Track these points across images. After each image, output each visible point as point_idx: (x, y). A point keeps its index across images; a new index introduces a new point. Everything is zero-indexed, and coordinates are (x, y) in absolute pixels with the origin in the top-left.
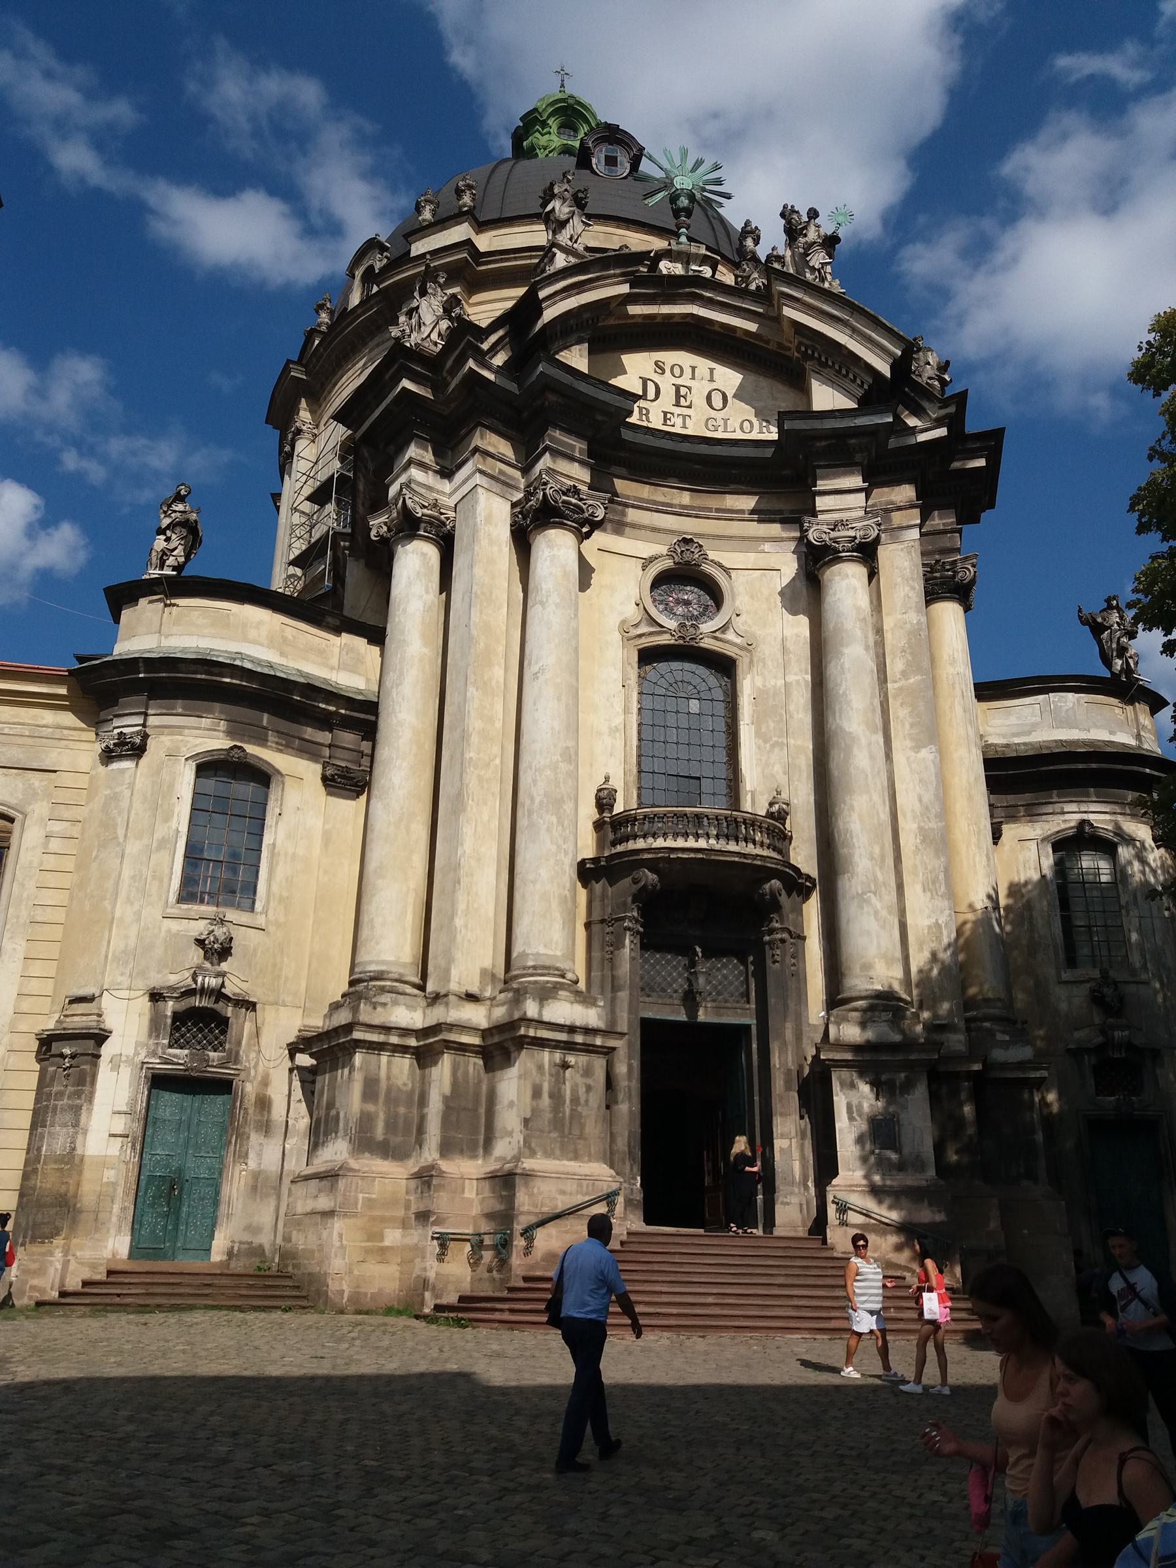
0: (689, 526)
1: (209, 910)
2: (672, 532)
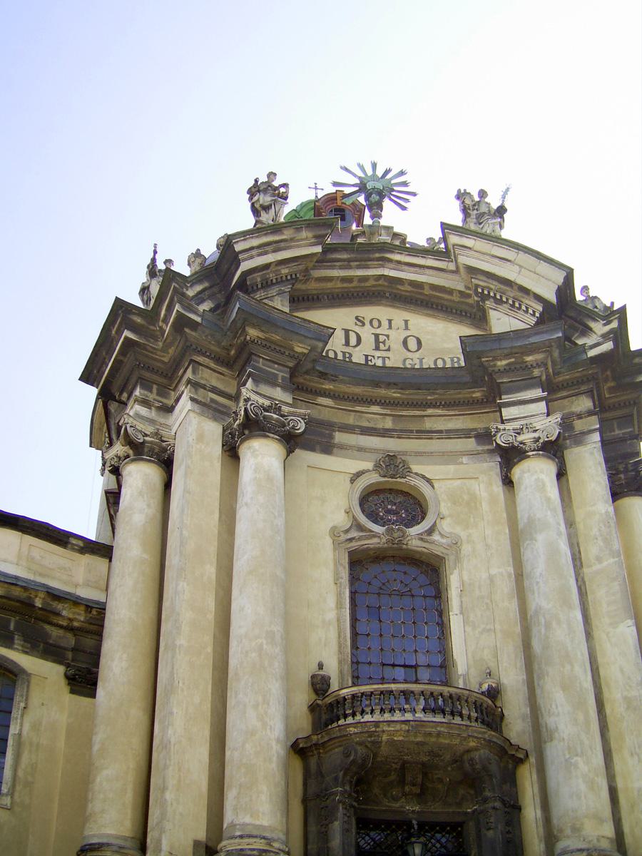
0: (392, 444)
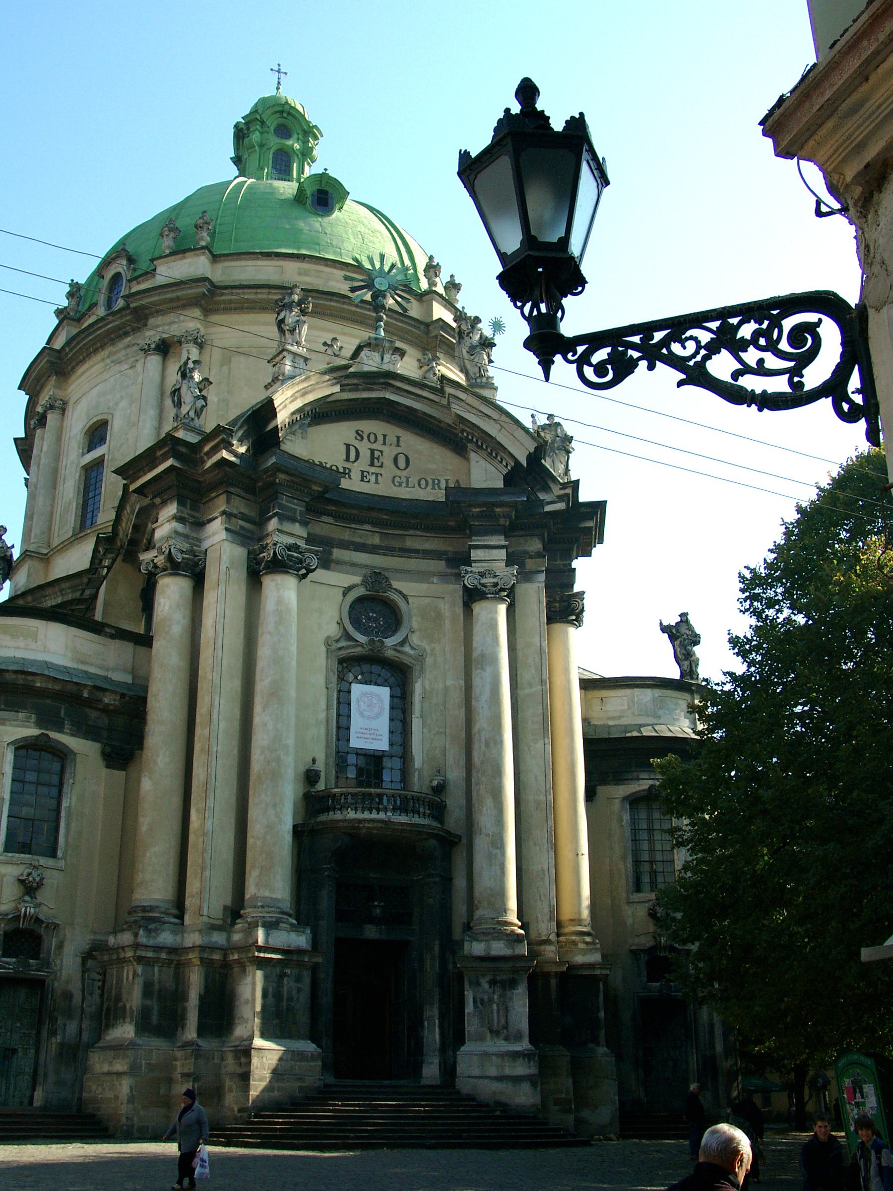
2: (365, 566)
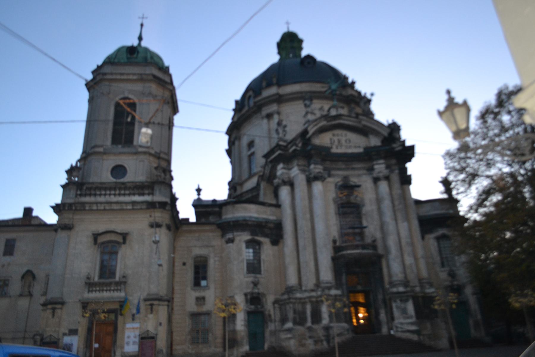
1: (253, 275)
